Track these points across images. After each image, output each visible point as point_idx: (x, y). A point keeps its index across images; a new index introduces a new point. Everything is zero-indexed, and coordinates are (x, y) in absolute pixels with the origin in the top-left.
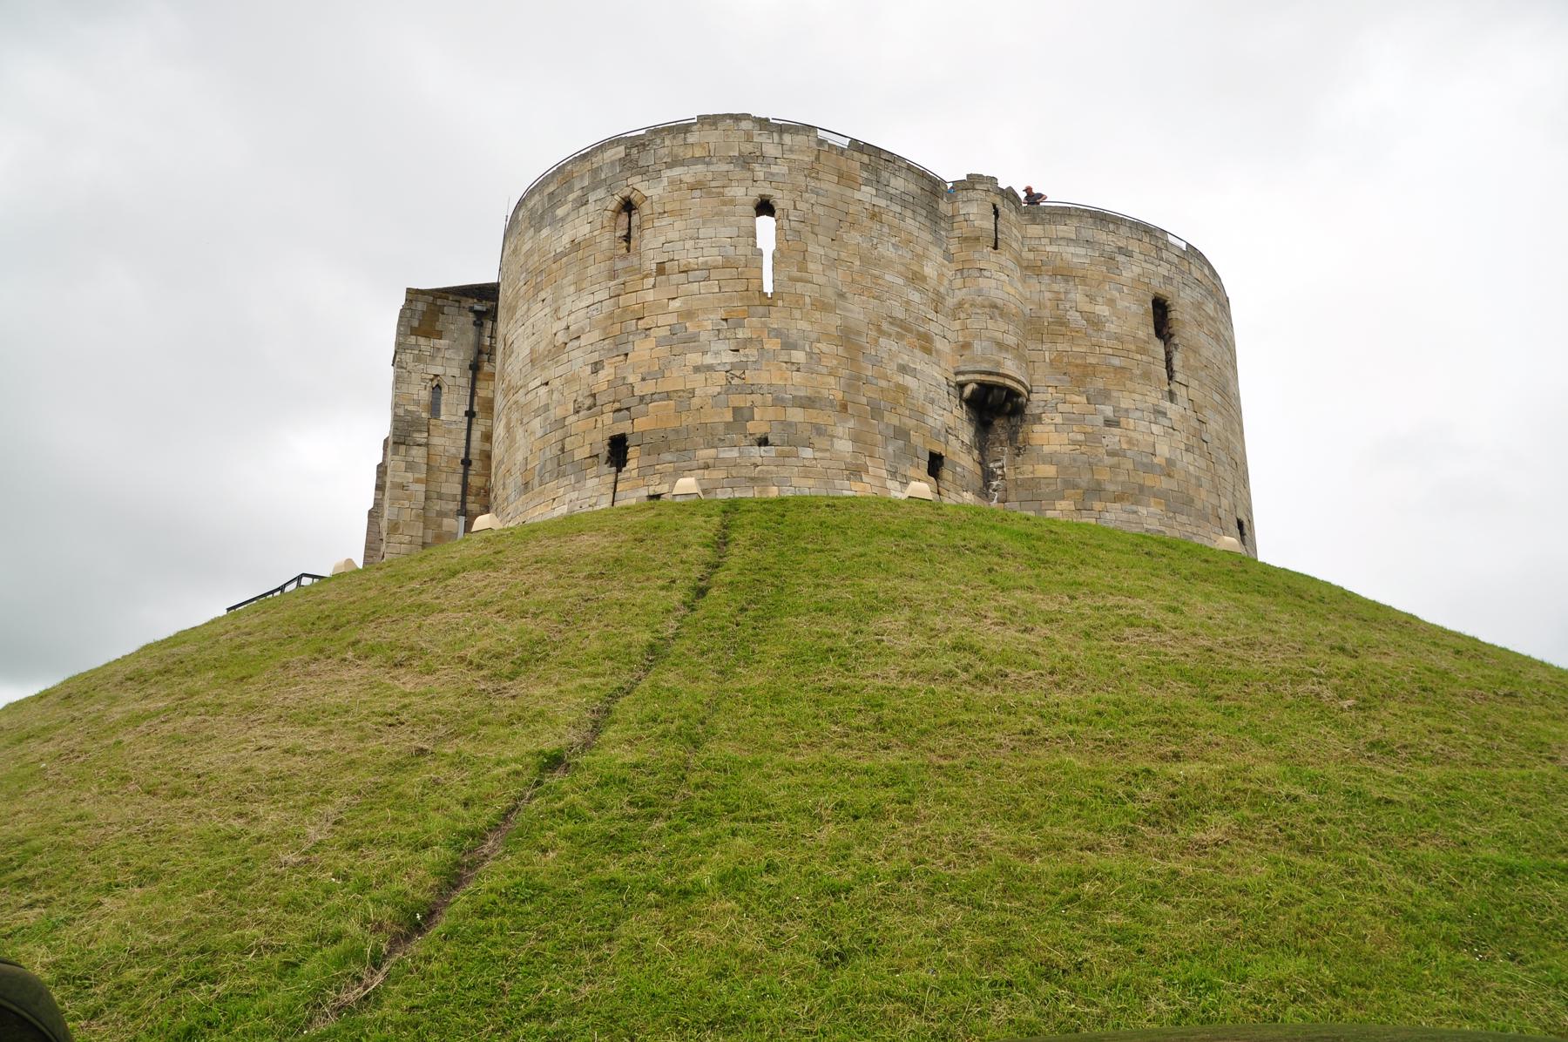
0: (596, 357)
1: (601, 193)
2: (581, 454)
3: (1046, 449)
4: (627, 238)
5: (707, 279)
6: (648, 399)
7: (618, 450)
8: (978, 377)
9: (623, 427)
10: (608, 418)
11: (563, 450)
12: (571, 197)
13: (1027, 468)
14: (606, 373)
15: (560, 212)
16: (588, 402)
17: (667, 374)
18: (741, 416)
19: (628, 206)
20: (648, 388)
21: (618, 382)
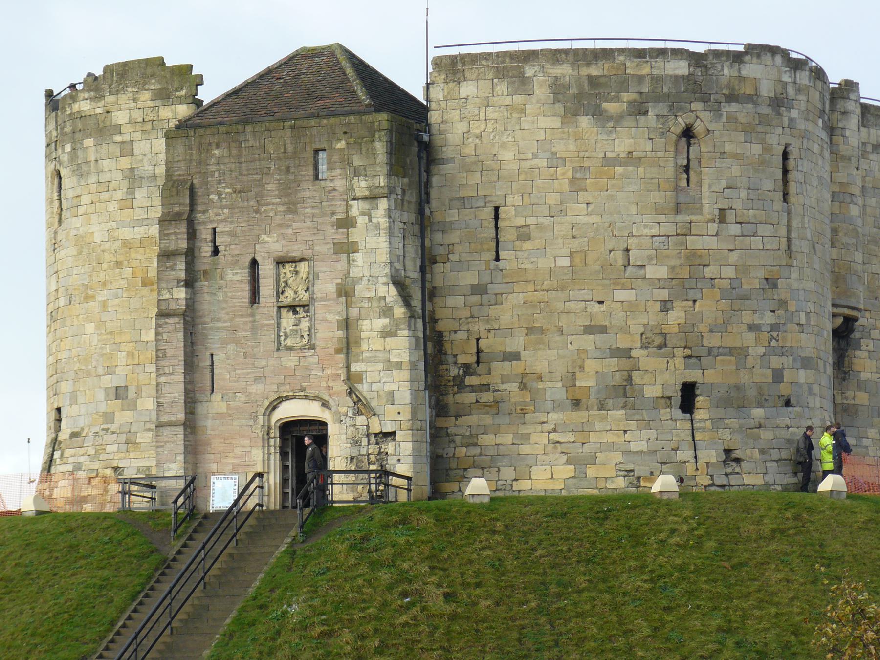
0: (664, 294)
1: (663, 108)
2: (652, 391)
3: (864, 376)
4: (687, 169)
5: (755, 234)
6: (715, 351)
7: (688, 397)
8: (847, 312)
9: (693, 375)
10: (679, 362)
11: (630, 379)
12: (625, 97)
13: (850, 394)
14: (676, 317)
15: (611, 107)
16: (658, 340)
17: (730, 329)
18: (778, 376)
19: (688, 133)
20: (713, 341)
21: (686, 329)
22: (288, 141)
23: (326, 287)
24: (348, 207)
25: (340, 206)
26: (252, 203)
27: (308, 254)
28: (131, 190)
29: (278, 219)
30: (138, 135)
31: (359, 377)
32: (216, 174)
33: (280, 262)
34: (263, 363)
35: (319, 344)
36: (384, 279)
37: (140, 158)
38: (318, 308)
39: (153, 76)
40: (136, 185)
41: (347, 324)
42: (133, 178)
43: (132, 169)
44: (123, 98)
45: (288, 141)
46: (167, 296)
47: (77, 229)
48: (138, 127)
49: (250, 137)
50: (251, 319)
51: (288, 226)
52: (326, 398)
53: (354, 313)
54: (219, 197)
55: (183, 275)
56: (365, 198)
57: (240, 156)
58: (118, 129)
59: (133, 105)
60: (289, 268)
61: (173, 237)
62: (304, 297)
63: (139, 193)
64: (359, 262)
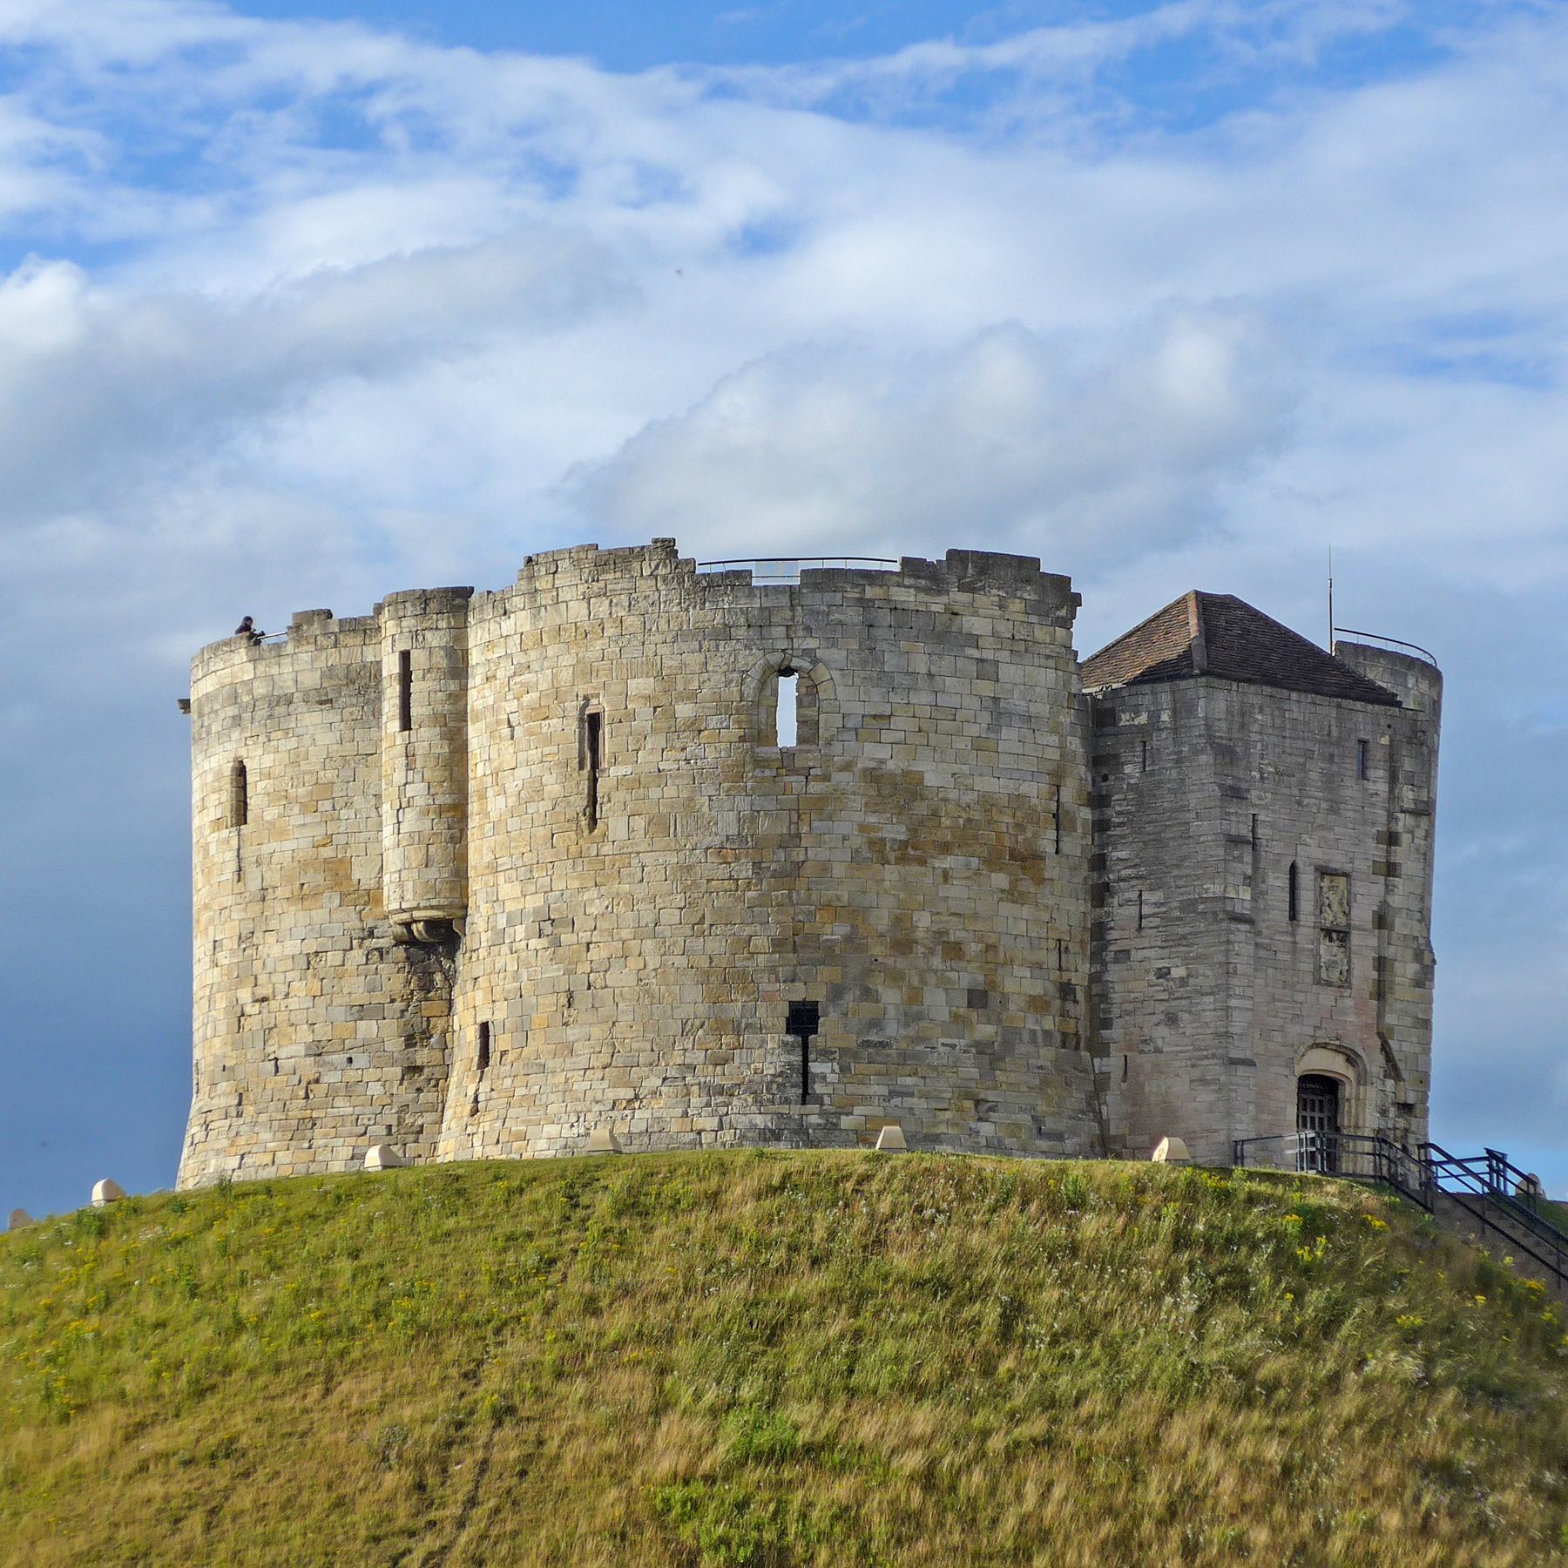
22: (1333, 722)
23: (1363, 914)
24: (1391, 818)
25: (1381, 816)
26: (1295, 791)
27: (1348, 868)
28: (995, 727)
29: (1320, 819)
30: (1004, 655)
31: (1391, 1029)
32: (1259, 746)
33: (1323, 872)
34: (1300, 997)
35: (1354, 981)
36: (1418, 916)
37: (1009, 687)
38: (1356, 939)
39: (1028, 582)
40: (1002, 721)
41: (1381, 964)
42: (998, 713)
43: (995, 699)
44: (986, 601)
45: (1333, 722)
46: (1232, 895)
47: (882, 762)
48: (1007, 644)
49: (1295, 707)
50: (1289, 939)
51: (1331, 829)
52: (1360, 1052)
53: (1390, 952)
54: (1262, 778)
55: (1249, 872)
56: (1411, 812)
57: (1283, 728)
58: (974, 640)
59: (998, 613)
60: (1326, 883)
61: (1234, 818)
62: (1342, 920)
63: (1005, 733)
64: (1399, 890)
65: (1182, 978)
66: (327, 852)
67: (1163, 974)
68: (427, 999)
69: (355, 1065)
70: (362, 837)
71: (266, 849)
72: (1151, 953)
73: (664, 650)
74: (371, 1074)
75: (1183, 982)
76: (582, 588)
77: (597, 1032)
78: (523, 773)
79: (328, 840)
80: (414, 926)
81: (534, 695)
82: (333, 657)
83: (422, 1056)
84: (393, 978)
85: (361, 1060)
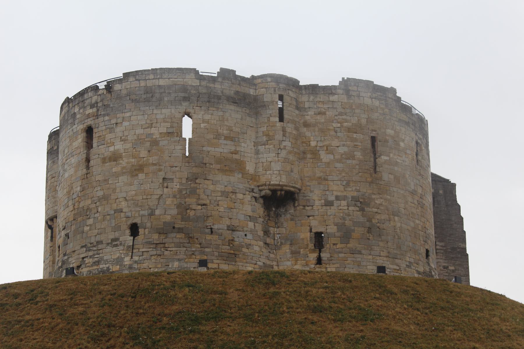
65: (453, 270)
66: (236, 157)
67: (446, 268)
68: (269, 220)
69: (248, 237)
70: (249, 155)
71: (204, 148)
72: (441, 261)
73: (396, 123)
74: (253, 242)
75: (453, 271)
76: (369, 94)
77: (381, 244)
78: (346, 149)
79: (236, 152)
80: (279, 193)
81: (350, 124)
82: (238, 89)
83: (268, 240)
84: (260, 210)
85: (250, 236)
